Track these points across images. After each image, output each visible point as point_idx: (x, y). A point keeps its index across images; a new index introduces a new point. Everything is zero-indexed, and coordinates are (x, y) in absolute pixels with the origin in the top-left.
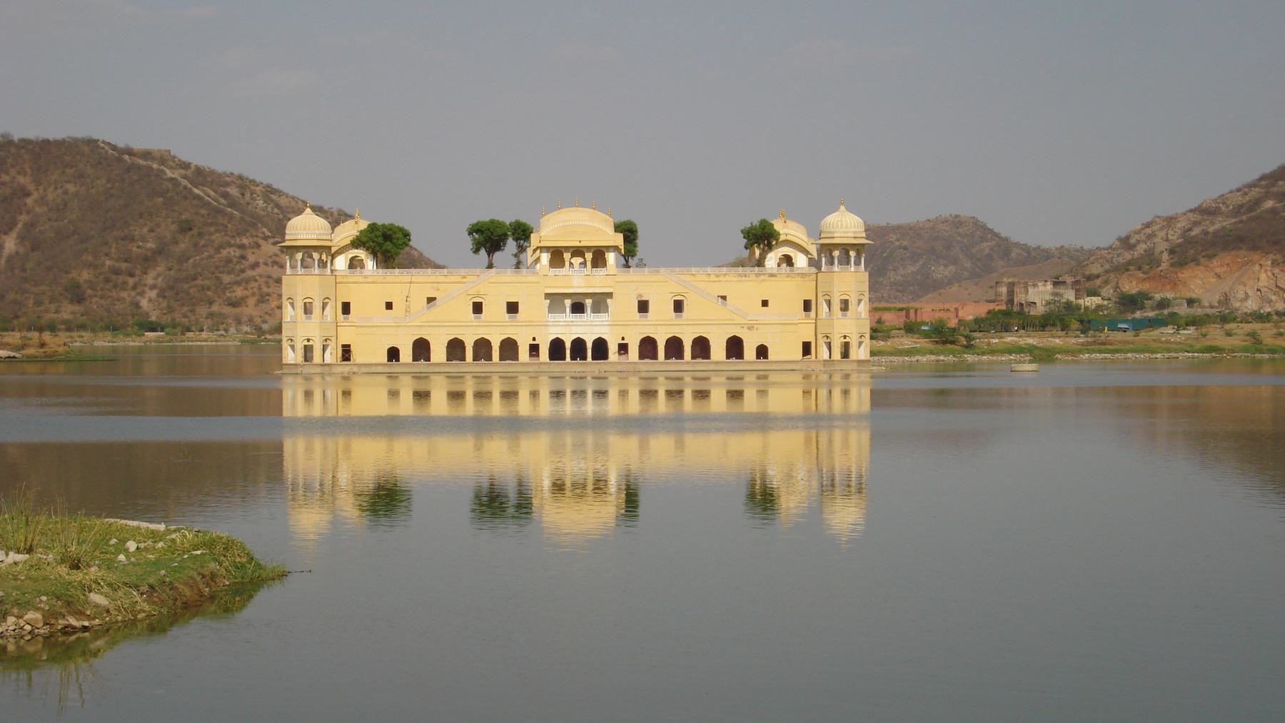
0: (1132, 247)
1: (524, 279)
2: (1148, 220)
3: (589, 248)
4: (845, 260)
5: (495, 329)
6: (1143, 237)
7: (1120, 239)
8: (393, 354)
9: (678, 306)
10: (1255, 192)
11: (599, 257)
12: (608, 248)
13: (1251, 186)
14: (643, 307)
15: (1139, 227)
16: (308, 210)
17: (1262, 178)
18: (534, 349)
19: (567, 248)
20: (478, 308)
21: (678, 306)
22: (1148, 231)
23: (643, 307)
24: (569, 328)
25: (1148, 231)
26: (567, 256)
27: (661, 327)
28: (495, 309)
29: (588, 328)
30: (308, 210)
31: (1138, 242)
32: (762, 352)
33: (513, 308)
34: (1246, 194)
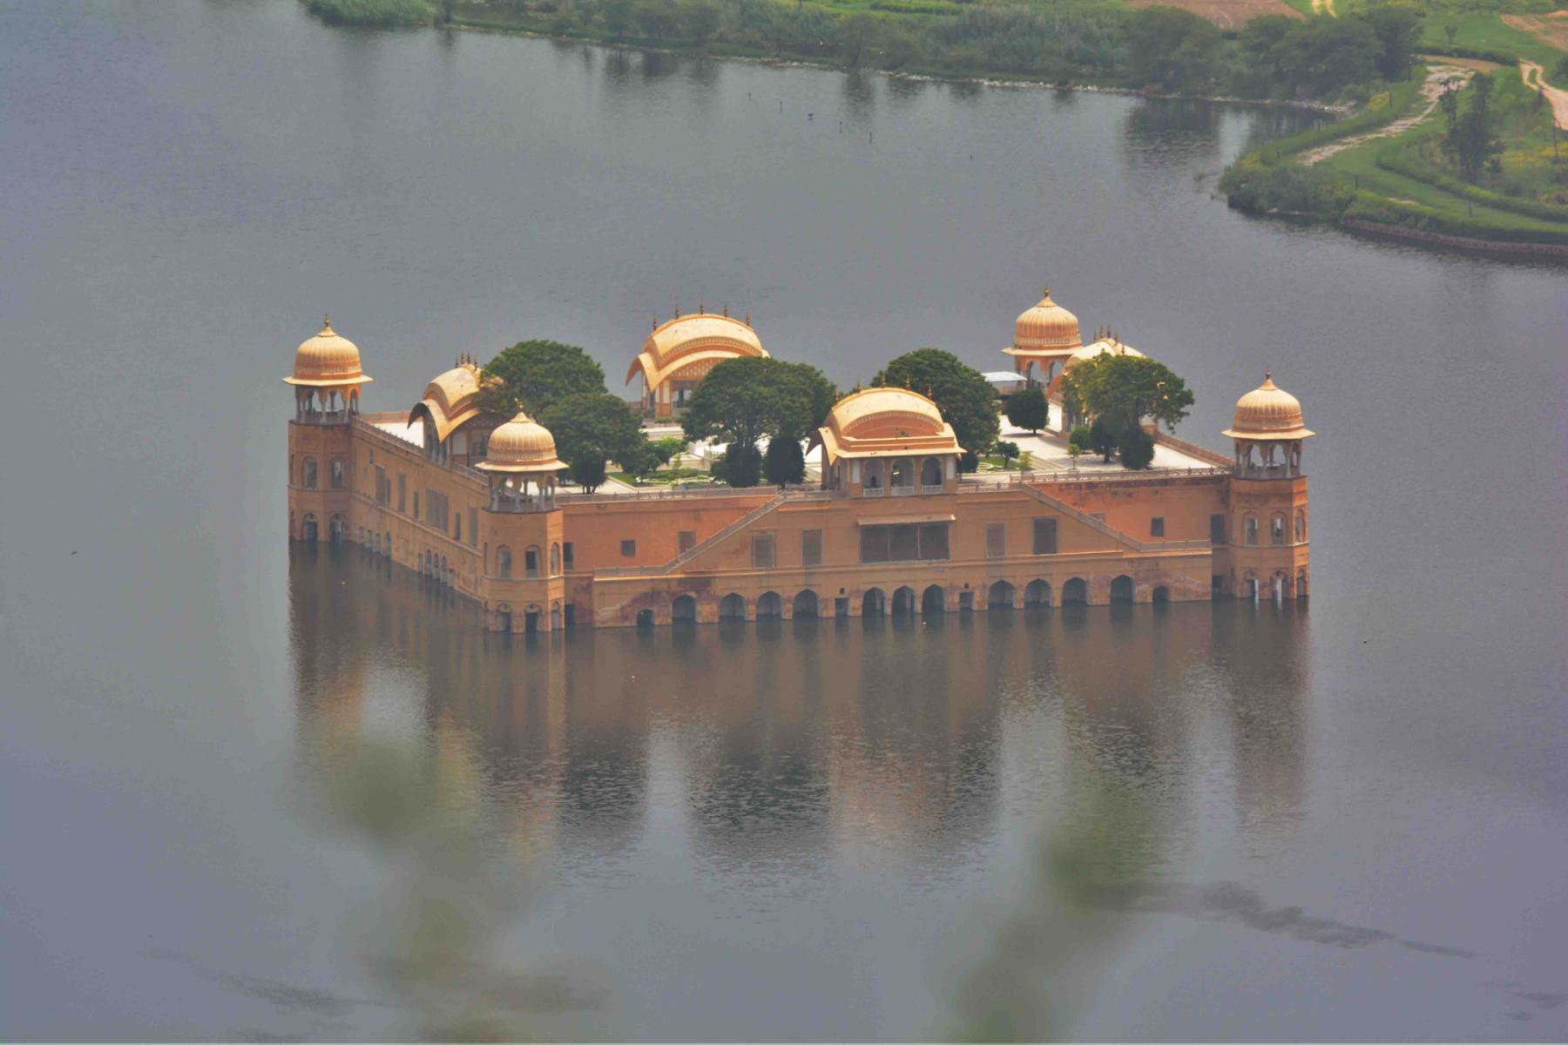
18: (841, 603)
21: (1045, 535)
24: (888, 577)
27: (1021, 564)
29: (916, 575)
33: (812, 548)
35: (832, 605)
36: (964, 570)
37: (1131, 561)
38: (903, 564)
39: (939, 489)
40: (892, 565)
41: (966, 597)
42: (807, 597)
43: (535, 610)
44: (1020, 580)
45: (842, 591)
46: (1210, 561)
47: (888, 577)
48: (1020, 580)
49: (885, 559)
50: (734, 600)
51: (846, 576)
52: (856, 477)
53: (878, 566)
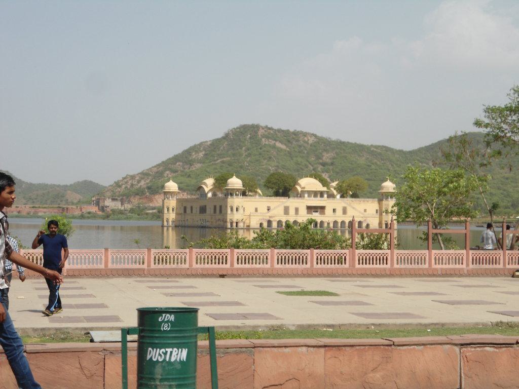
0: (120, 186)
1: (257, 200)
2: (124, 176)
4: (391, 197)
6: (124, 183)
7: (115, 182)
9: (345, 211)
10: (161, 168)
11: (322, 194)
13: (159, 165)
14: (334, 210)
15: (121, 179)
16: (234, 177)
17: (163, 162)
20: (286, 211)
21: (345, 211)
22: (126, 180)
23: (334, 210)
25: (126, 180)
28: (292, 211)
30: (234, 177)
31: (122, 185)
33: (297, 210)
34: (158, 168)
36: (328, 218)
37: (362, 217)
39: (323, 199)
44: (339, 221)
46: (378, 219)
48: (339, 221)
50: (279, 222)
51: (303, 217)
52: (306, 195)
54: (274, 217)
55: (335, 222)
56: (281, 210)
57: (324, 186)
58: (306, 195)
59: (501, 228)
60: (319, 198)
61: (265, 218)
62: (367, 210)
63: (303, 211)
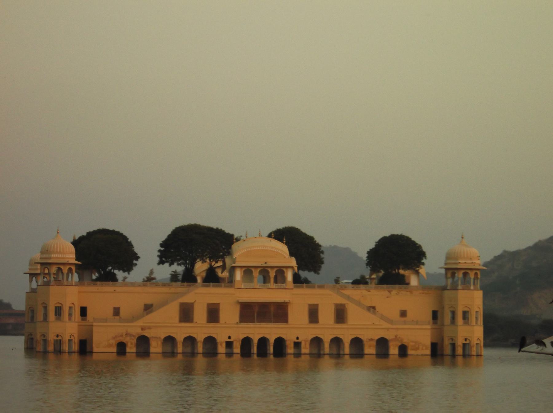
3: (272, 267)
5: (200, 329)
8: (121, 348)
9: (340, 315)
12: (287, 267)
14: (313, 314)
18: (229, 345)
19: (256, 267)
20: (186, 313)
21: (340, 315)
24: (256, 331)
26: (256, 273)
27: (327, 329)
32: (403, 350)
35: (224, 345)
37: (388, 329)
38: (263, 325)
40: (257, 325)
41: (297, 345)
42: (211, 341)
43: (59, 338)
45: (230, 337)
47: (256, 331)
49: (254, 322)
50: (170, 340)
53: (251, 325)
54: (150, 328)
55: (317, 341)
56: (172, 311)
57: (291, 254)
58: (238, 275)
59: (42, 350)
60: (272, 284)
61: (131, 331)
62: (409, 314)
63: (229, 314)
